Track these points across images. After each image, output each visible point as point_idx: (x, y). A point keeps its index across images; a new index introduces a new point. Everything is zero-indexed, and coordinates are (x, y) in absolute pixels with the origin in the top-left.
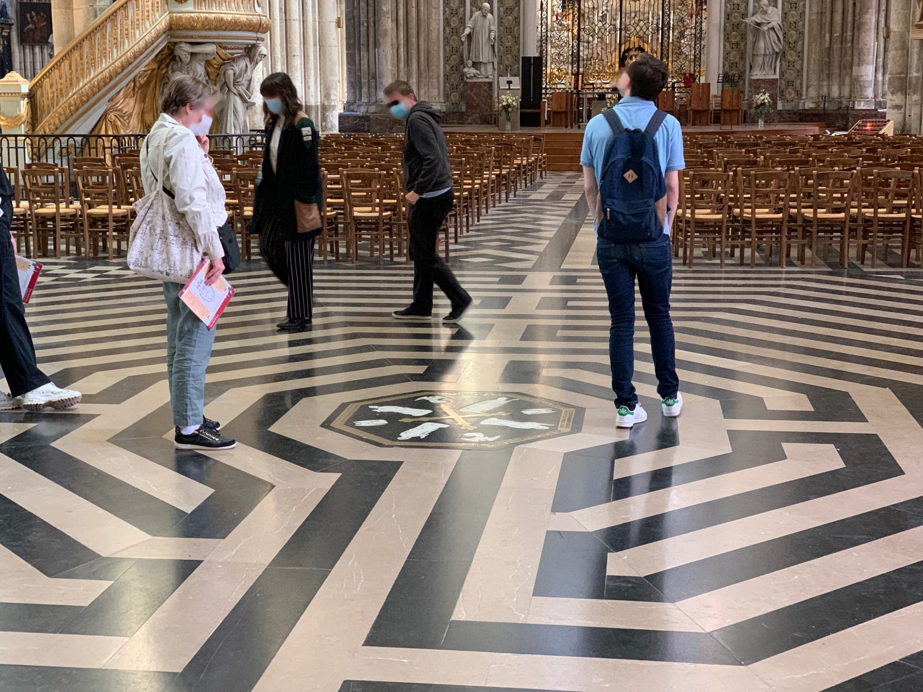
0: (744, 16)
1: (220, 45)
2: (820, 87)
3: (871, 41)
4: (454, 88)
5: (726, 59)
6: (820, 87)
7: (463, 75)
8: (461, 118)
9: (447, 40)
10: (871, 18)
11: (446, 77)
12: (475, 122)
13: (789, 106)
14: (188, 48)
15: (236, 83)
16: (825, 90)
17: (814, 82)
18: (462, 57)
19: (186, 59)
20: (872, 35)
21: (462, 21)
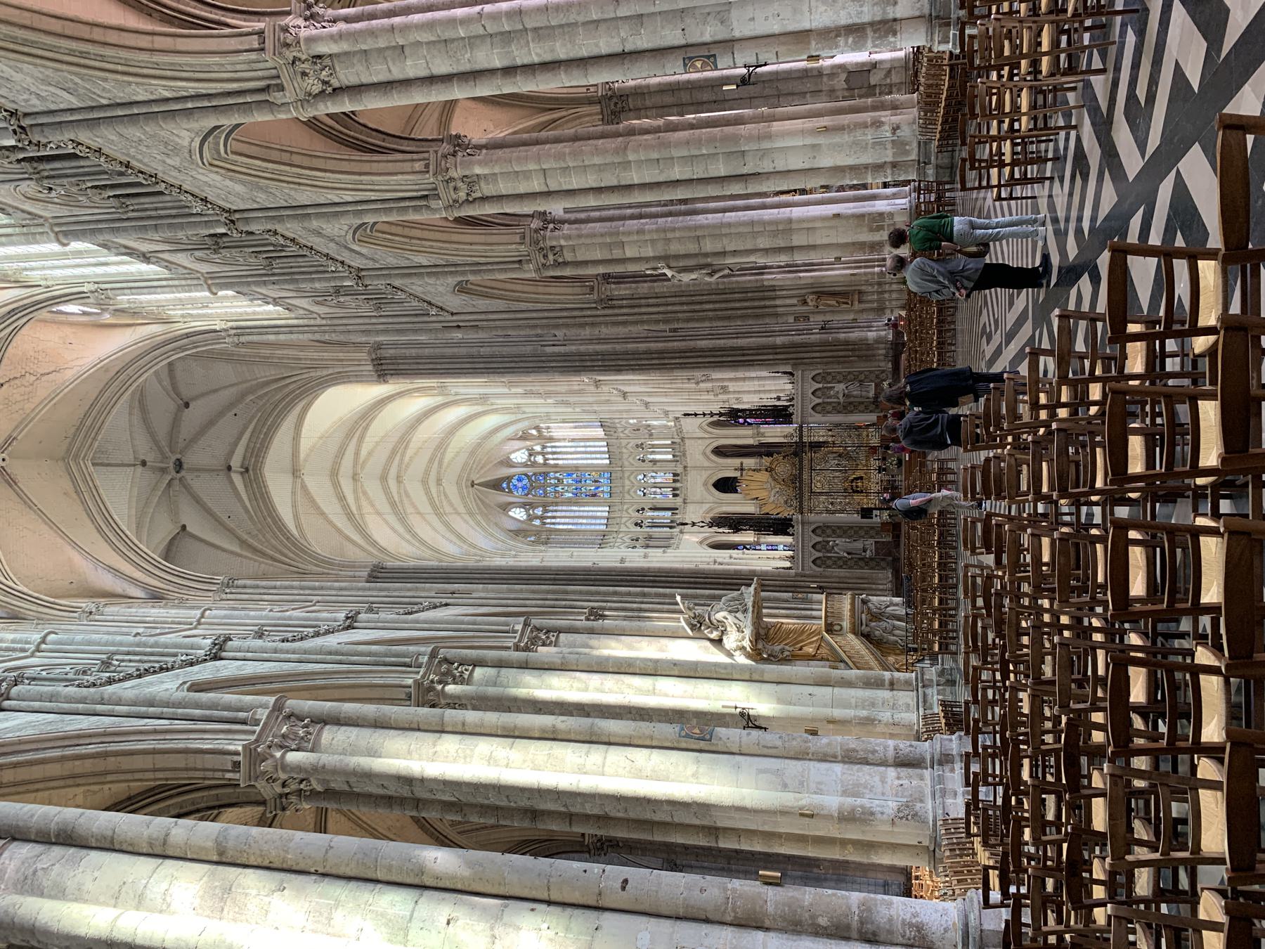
0: (839, 403)
1: (863, 612)
2: (879, 360)
3: (855, 335)
4: (878, 564)
5: (863, 412)
6: (879, 360)
7: (871, 559)
8: (896, 560)
9: (851, 568)
10: (842, 336)
11: (872, 568)
12: (899, 552)
13: (890, 376)
14: (864, 627)
15: (880, 609)
16: (882, 358)
17: (876, 364)
18: (860, 559)
19: (868, 629)
20: (851, 335)
21: (840, 558)
